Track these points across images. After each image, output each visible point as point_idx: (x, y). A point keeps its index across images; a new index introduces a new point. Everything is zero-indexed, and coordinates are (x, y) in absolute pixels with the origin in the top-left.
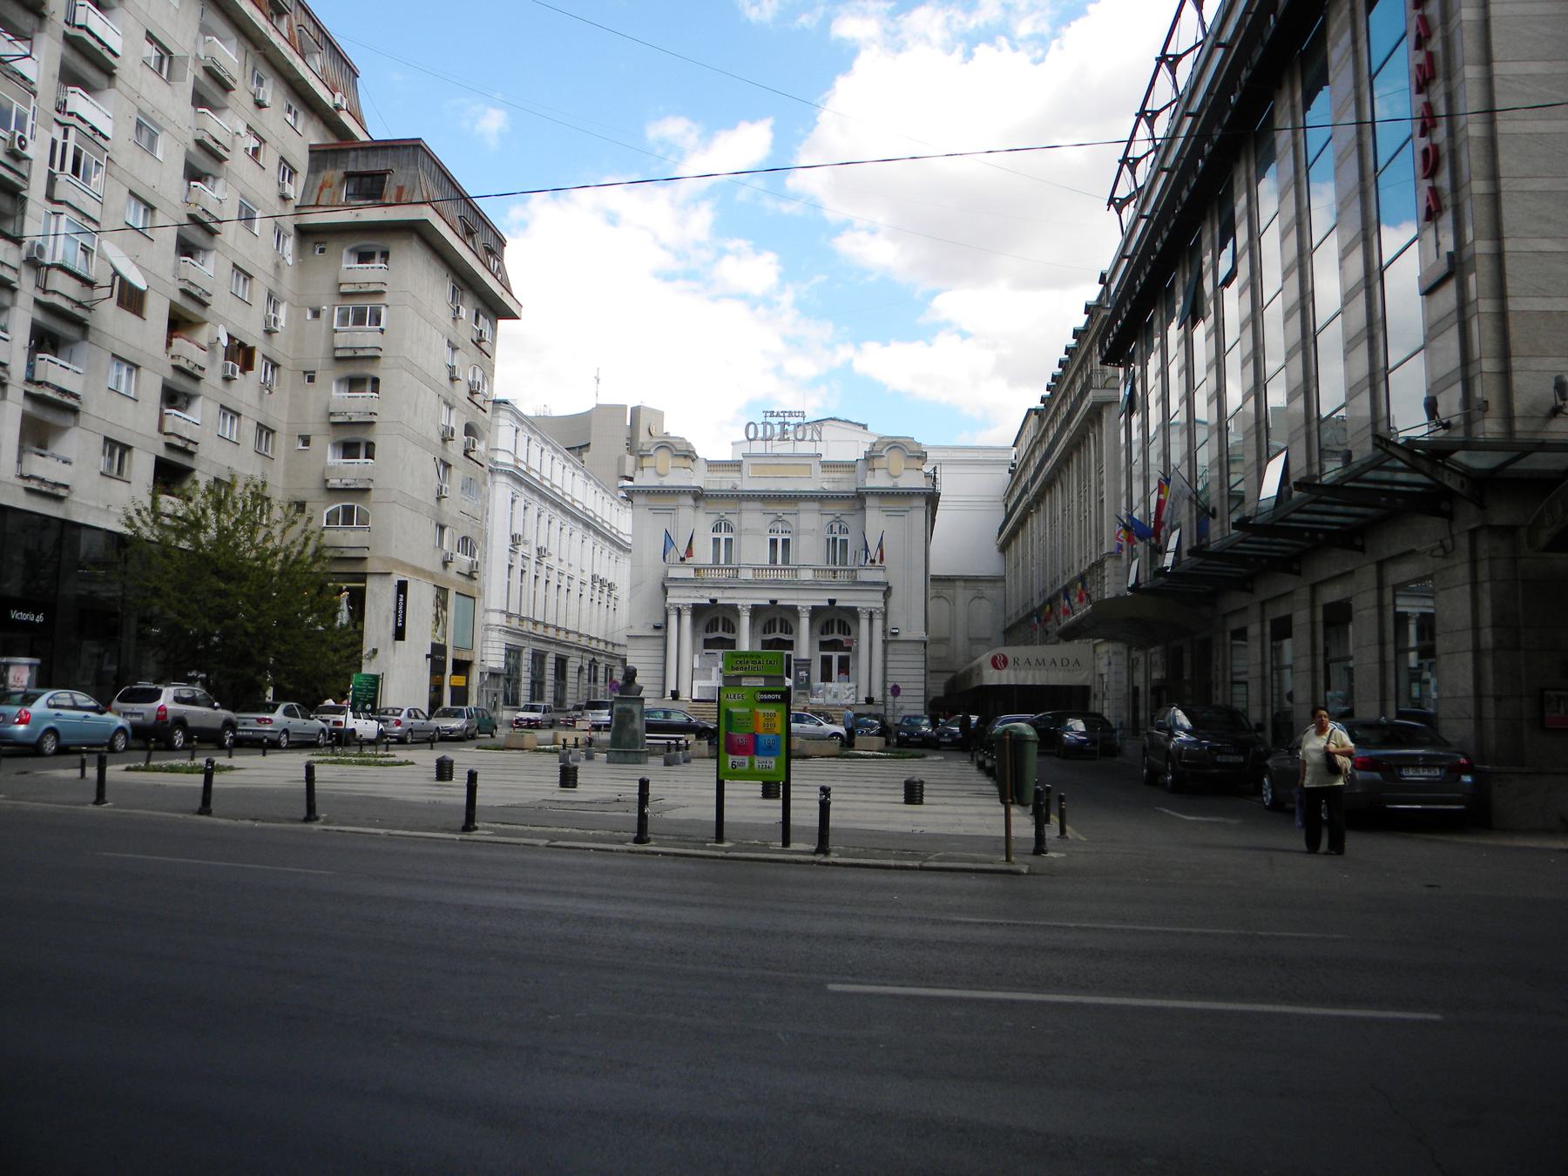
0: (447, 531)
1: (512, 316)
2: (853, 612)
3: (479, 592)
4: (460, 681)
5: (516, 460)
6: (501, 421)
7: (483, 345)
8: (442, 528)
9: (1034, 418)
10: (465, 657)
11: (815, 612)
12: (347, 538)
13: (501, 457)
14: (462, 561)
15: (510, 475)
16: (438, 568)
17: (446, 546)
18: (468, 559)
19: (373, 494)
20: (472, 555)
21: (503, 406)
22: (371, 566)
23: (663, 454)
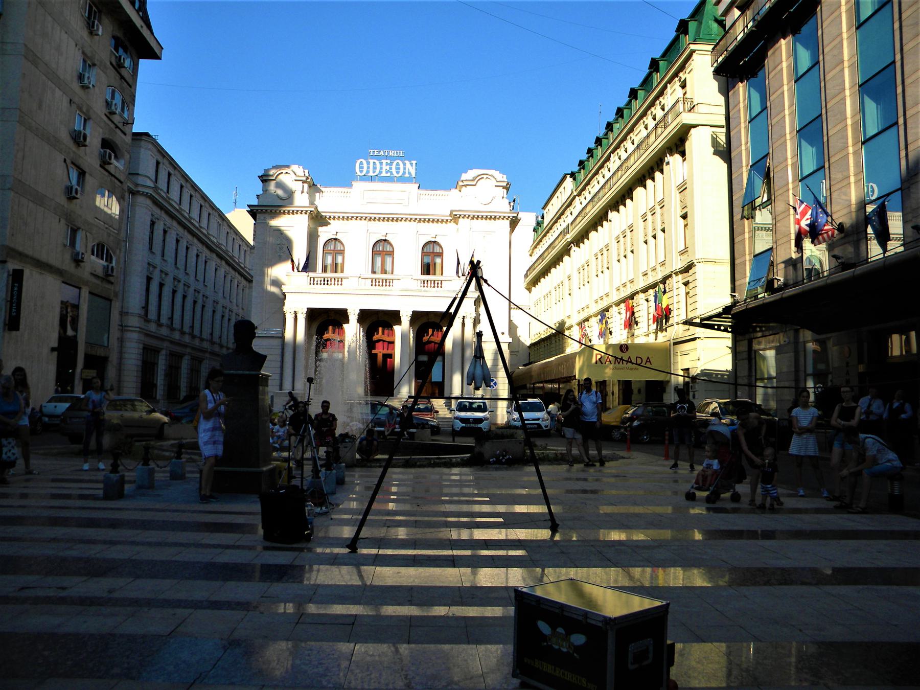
0: (80, 236)
1: (153, 55)
3: (116, 295)
4: (92, 373)
5: (156, 189)
6: (142, 150)
8: (74, 231)
9: (569, 179)
10: (101, 352)
13: (140, 180)
15: (147, 195)
16: (67, 265)
17: (79, 247)
18: (104, 263)
20: (109, 259)
21: (144, 138)
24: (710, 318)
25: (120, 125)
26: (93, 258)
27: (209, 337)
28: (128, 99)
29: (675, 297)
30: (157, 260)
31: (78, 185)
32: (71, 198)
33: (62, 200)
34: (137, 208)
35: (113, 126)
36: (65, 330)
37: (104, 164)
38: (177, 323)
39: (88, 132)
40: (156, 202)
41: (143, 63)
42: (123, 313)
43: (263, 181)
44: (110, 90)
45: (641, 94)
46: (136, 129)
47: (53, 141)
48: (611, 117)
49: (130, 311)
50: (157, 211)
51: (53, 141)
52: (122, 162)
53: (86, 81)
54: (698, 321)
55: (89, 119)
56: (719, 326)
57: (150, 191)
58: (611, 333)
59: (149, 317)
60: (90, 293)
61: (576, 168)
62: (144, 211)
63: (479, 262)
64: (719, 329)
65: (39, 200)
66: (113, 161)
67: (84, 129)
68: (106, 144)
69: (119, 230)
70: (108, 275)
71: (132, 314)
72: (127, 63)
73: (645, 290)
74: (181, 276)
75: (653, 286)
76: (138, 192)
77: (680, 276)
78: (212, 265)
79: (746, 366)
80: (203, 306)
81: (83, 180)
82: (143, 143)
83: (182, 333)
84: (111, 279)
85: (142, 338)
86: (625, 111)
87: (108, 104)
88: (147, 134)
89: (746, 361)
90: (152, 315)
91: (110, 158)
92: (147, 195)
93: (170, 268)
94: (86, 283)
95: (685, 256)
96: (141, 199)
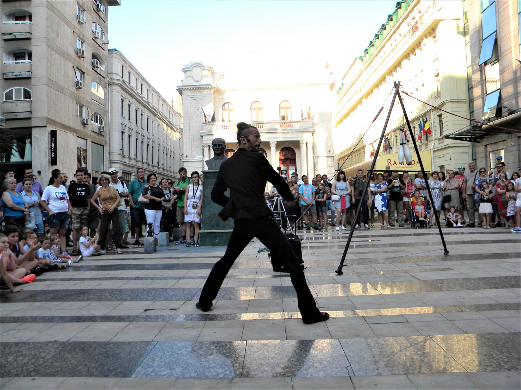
2: (297, 144)
3: (106, 143)
5: (123, 81)
6: (114, 59)
7: (100, 13)
8: (81, 107)
9: (359, 61)
11: (279, 144)
12: (20, 107)
13: (114, 77)
14: (94, 125)
15: (118, 85)
16: (79, 127)
17: (84, 116)
18: (98, 124)
19: (33, 81)
20: (101, 123)
21: (114, 52)
22: (34, 122)
23: (197, 70)
24: (461, 134)
25: (101, 45)
26: (92, 122)
27: (157, 165)
28: (104, 30)
29: (433, 123)
30: (126, 122)
31: (81, 80)
32: (78, 88)
33: (73, 89)
34: (114, 93)
35: (97, 45)
36: (81, 165)
37: (94, 68)
38: (139, 158)
39: (84, 50)
40: (123, 89)
41: (111, 8)
42: (110, 154)
43: (184, 72)
44: (94, 25)
45: (403, 5)
46: (110, 47)
47: (64, 55)
48: (384, 20)
49: (114, 151)
50: (124, 94)
51: (64, 55)
52: (104, 66)
53: (81, 20)
54: (454, 136)
55: (84, 42)
56: (466, 138)
57: (120, 82)
58: (391, 148)
59: (124, 154)
60: (92, 142)
61: (362, 53)
62: (117, 94)
63: (399, 82)
64: (466, 140)
65: (61, 90)
66: (99, 66)
67: (82, 47)
68: (94, 56)
69: (105, 105)
70: (101, 132)
71: (116, 154)
72: (102, 8)
73: (413, 121)
74: (140, 130)
75: (417, 119)
76: (113, 83)
77: (435, 112)
78: (155, 124)
79: (484, 162)
80: (153, 147)
81: (84, 77)
82: (114, 55)
83: (143, 163)
84: (103, 133)
85: (122, 166)
86: (394, 17)
87: (94, 33)
88: (116, 50)
89: (484, 158)
90: (126, 153)
91: (97, 64)
92: (118, 85)
93: (133, 126)
94: (90, 137)
95: (439, 99)
96: (115, 88)
